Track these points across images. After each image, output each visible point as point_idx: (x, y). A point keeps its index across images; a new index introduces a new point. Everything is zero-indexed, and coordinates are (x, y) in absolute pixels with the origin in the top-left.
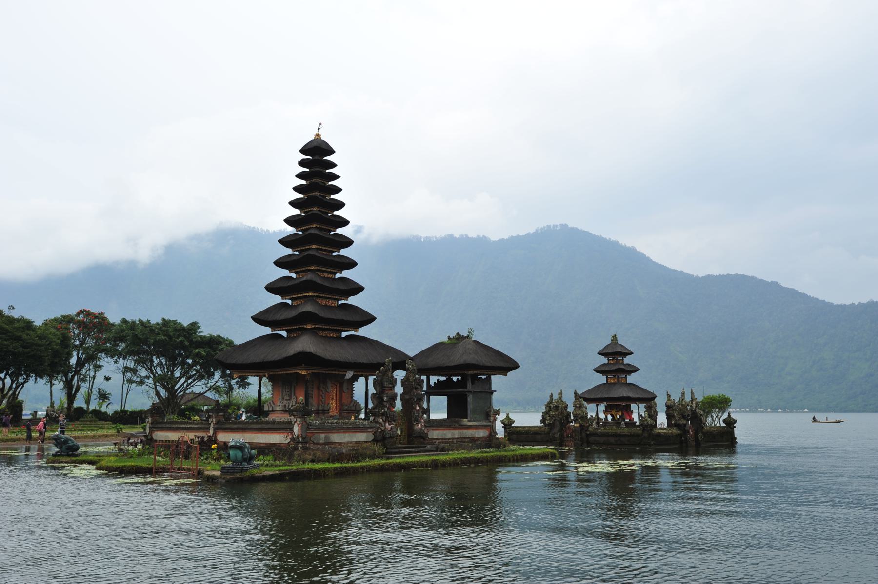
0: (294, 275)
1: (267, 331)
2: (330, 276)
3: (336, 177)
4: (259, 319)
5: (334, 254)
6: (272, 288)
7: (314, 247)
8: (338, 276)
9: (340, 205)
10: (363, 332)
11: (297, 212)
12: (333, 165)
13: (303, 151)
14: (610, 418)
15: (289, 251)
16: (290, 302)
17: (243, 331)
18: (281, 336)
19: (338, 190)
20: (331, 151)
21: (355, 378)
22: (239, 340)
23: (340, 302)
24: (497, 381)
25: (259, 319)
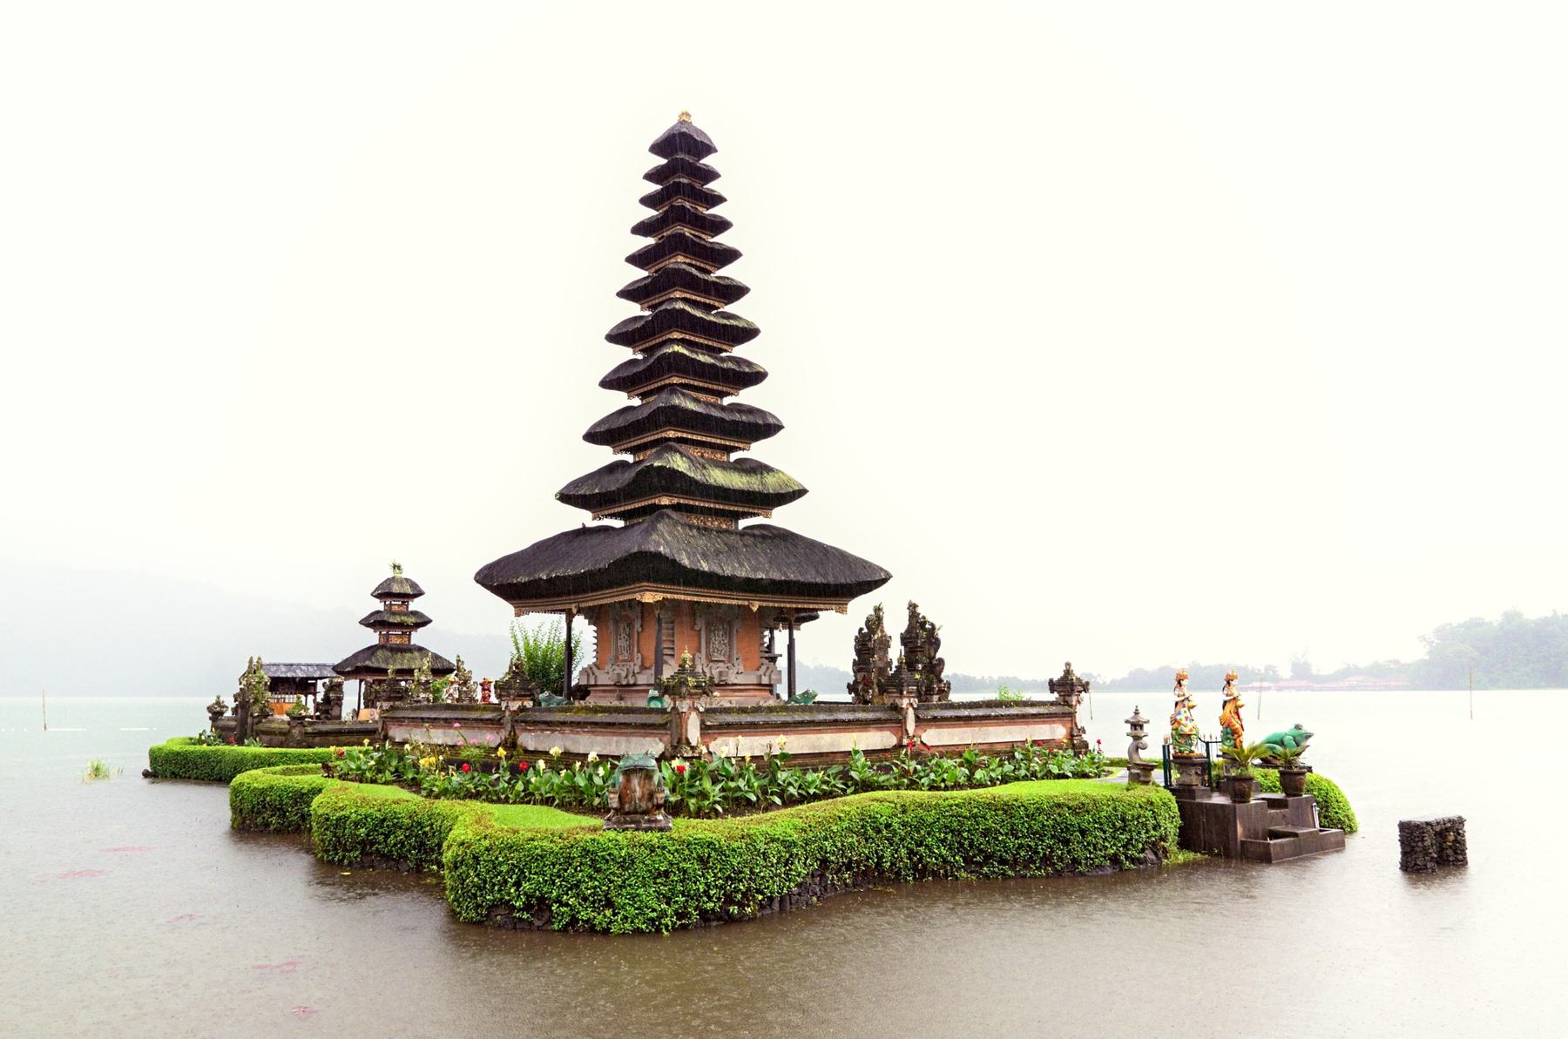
0: (636, 402)
10: (781, 518)
13: (657, 148)
16: (629, 458)
23: (734, 456)
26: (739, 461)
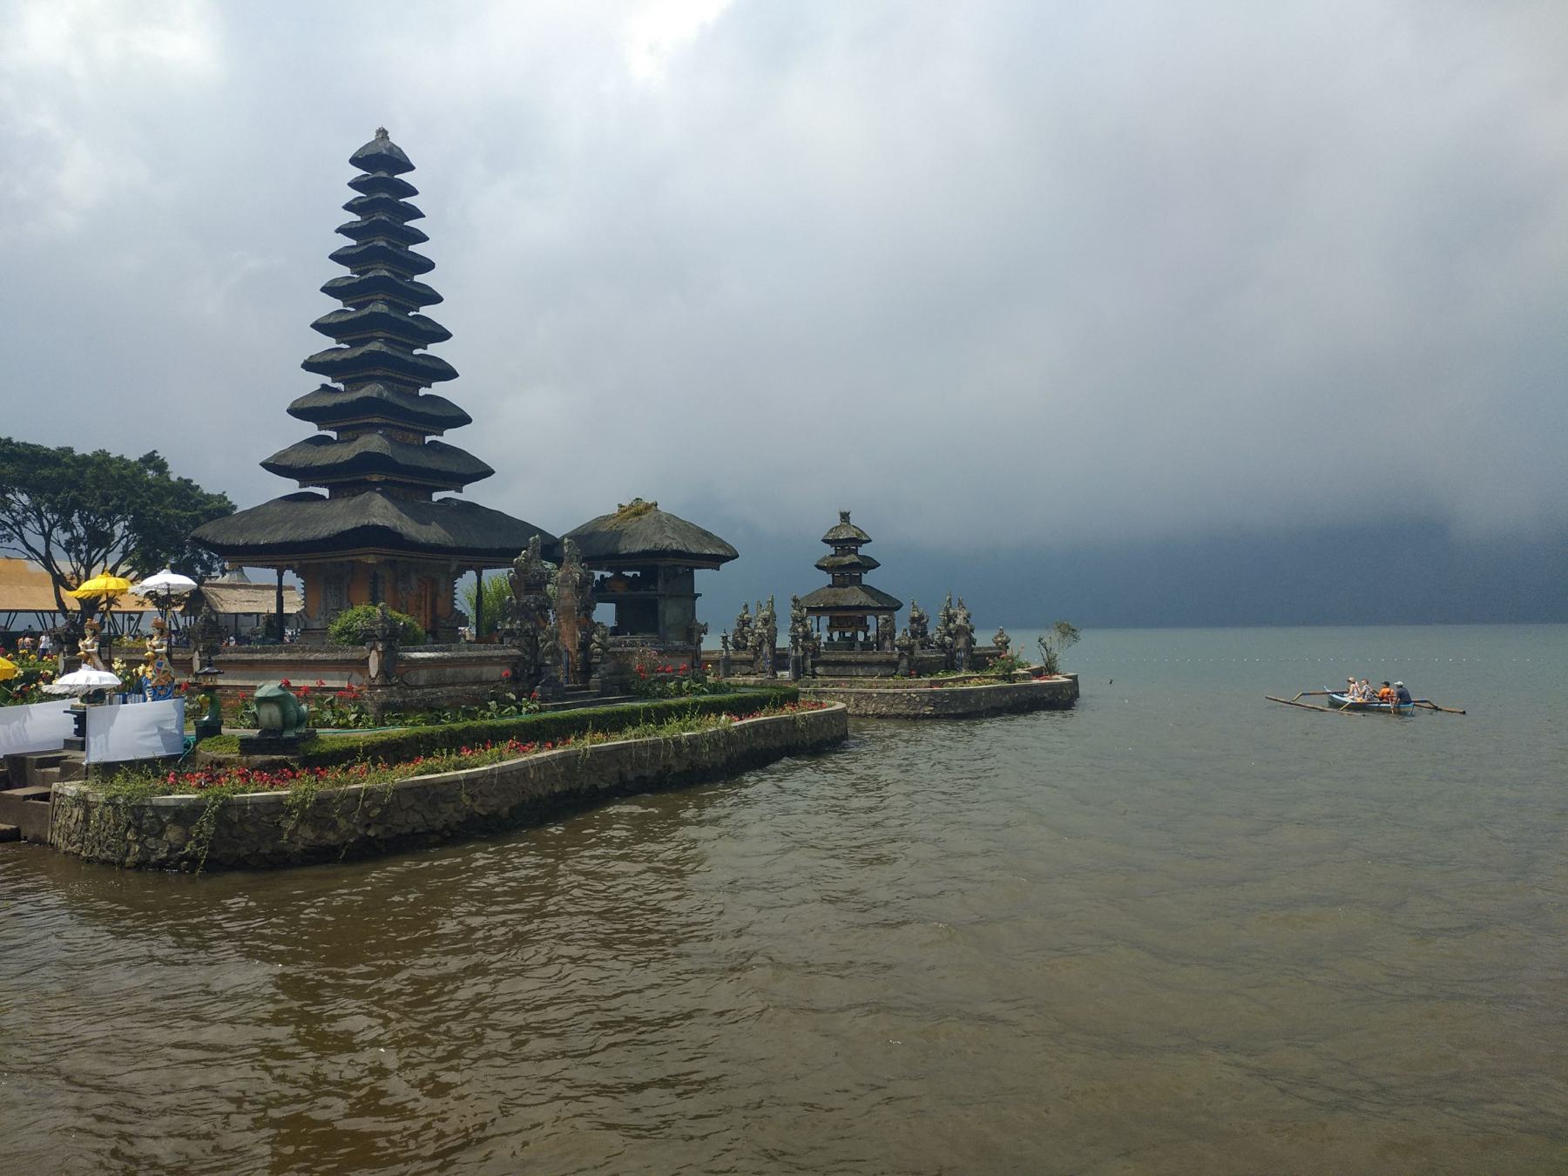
0: (341, 386)
1: (291, 486)
2: (410, 389)
3: (418, 214)
4: (275, 466)
5: (417, 352)
6: (300, 411)
7: (380, 334)
8: (423, 391)
9: (428, 266)
10: (473, 493)
11: (344, 271)
12: (413, 192)
13: (355, 161)
14: (836, 636)
15: (330, 343)
16: (334, 435)
17: (253, 489)
18: (322, 498)
19: (421, 238)
20: (411, 168)
21: (460, 573)
22: (244, 501)
23: (428, 439)
24: (702, 578)
25: (275, 466)
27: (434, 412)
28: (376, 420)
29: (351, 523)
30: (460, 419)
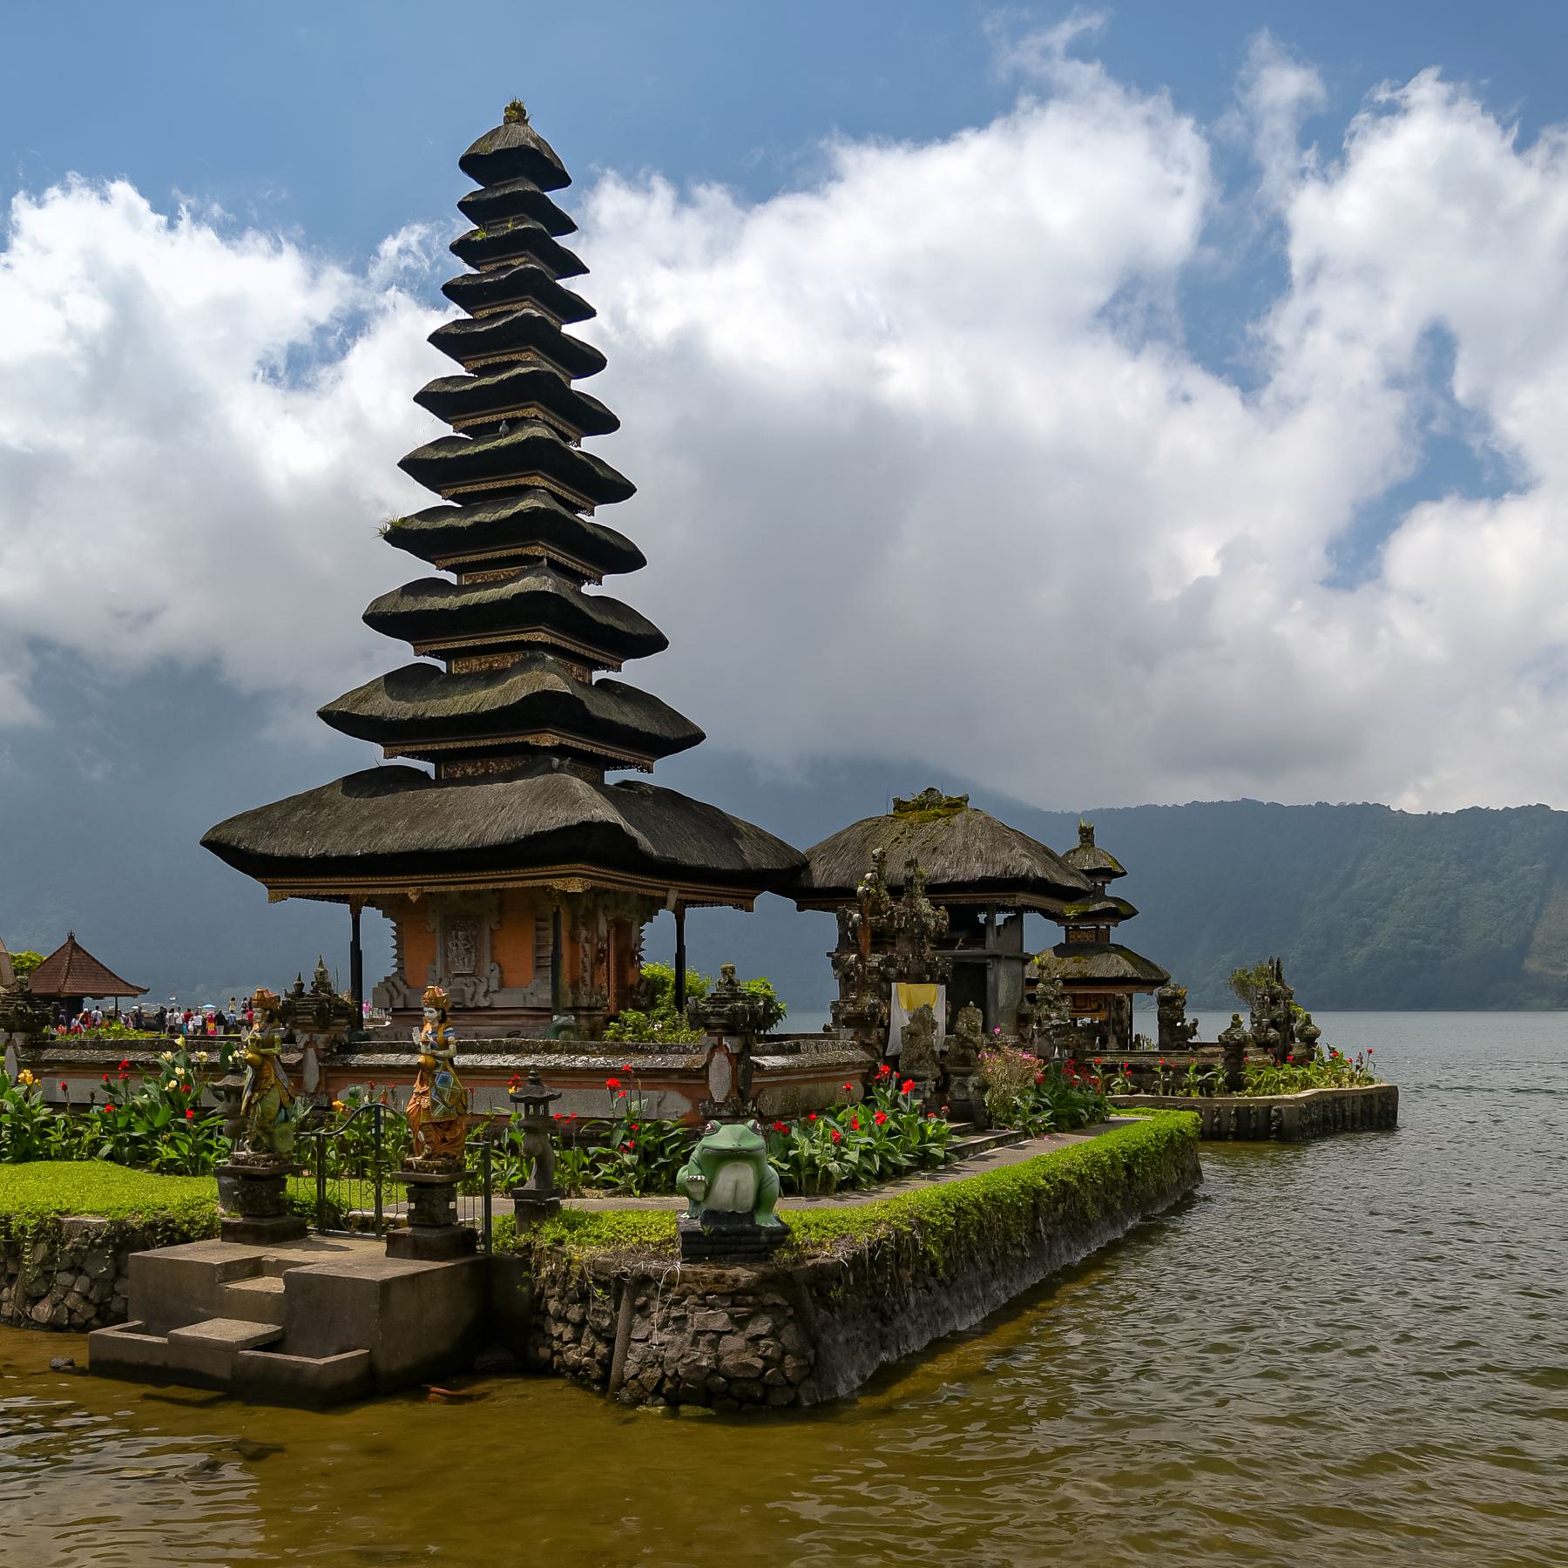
6: (382, 619)
8: (589, 589)
23: (597, 675)
26: (603, 683)
27: (622, 626)
28: (540, 637)
29: (556, 818)
30: (650, 642)
